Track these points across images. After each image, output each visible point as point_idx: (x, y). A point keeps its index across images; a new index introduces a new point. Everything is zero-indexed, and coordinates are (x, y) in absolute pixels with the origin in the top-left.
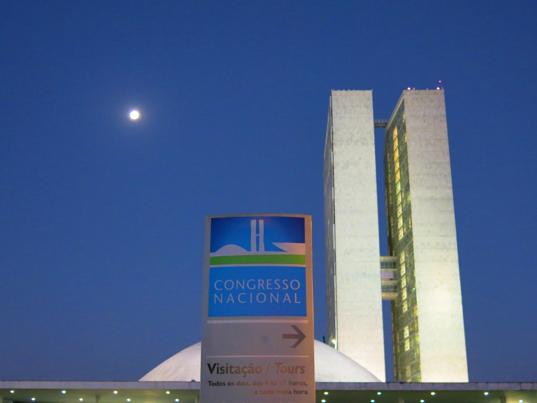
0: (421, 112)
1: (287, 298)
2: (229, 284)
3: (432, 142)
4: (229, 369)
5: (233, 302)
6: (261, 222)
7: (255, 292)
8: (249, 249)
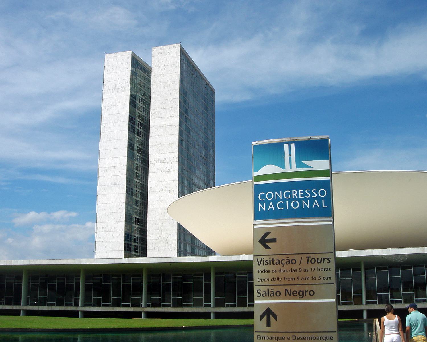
0: (163, 63)
1: (316, 204)
2: (270, 196)
3: (169, 83)
4: (271, 262)
5: (274, 209)
6: (293, 145)
7: (290, 201)
8: (283, 167)
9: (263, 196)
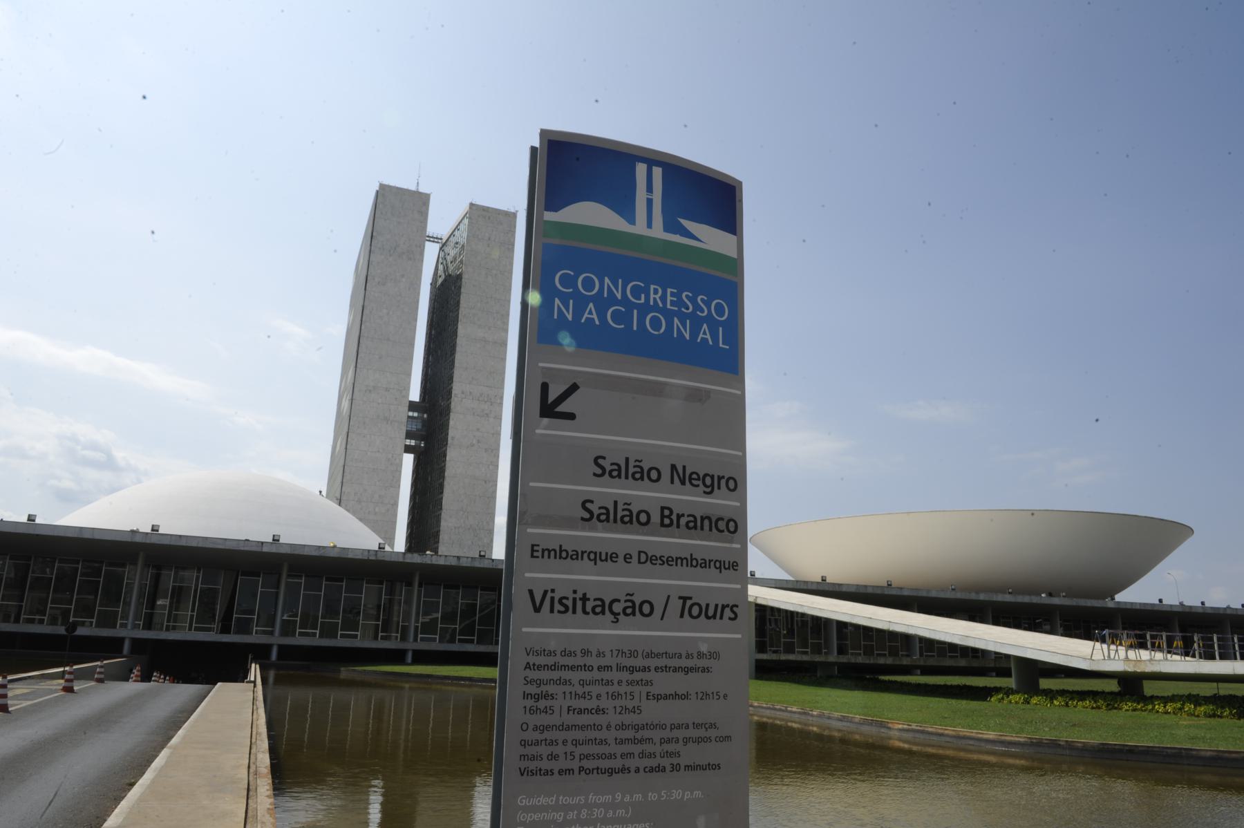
1: (705, 333)
2: (588, 284)
6: (657, 172)
7: (645, 309)
8: (632, 221)
9: (568, 281)
